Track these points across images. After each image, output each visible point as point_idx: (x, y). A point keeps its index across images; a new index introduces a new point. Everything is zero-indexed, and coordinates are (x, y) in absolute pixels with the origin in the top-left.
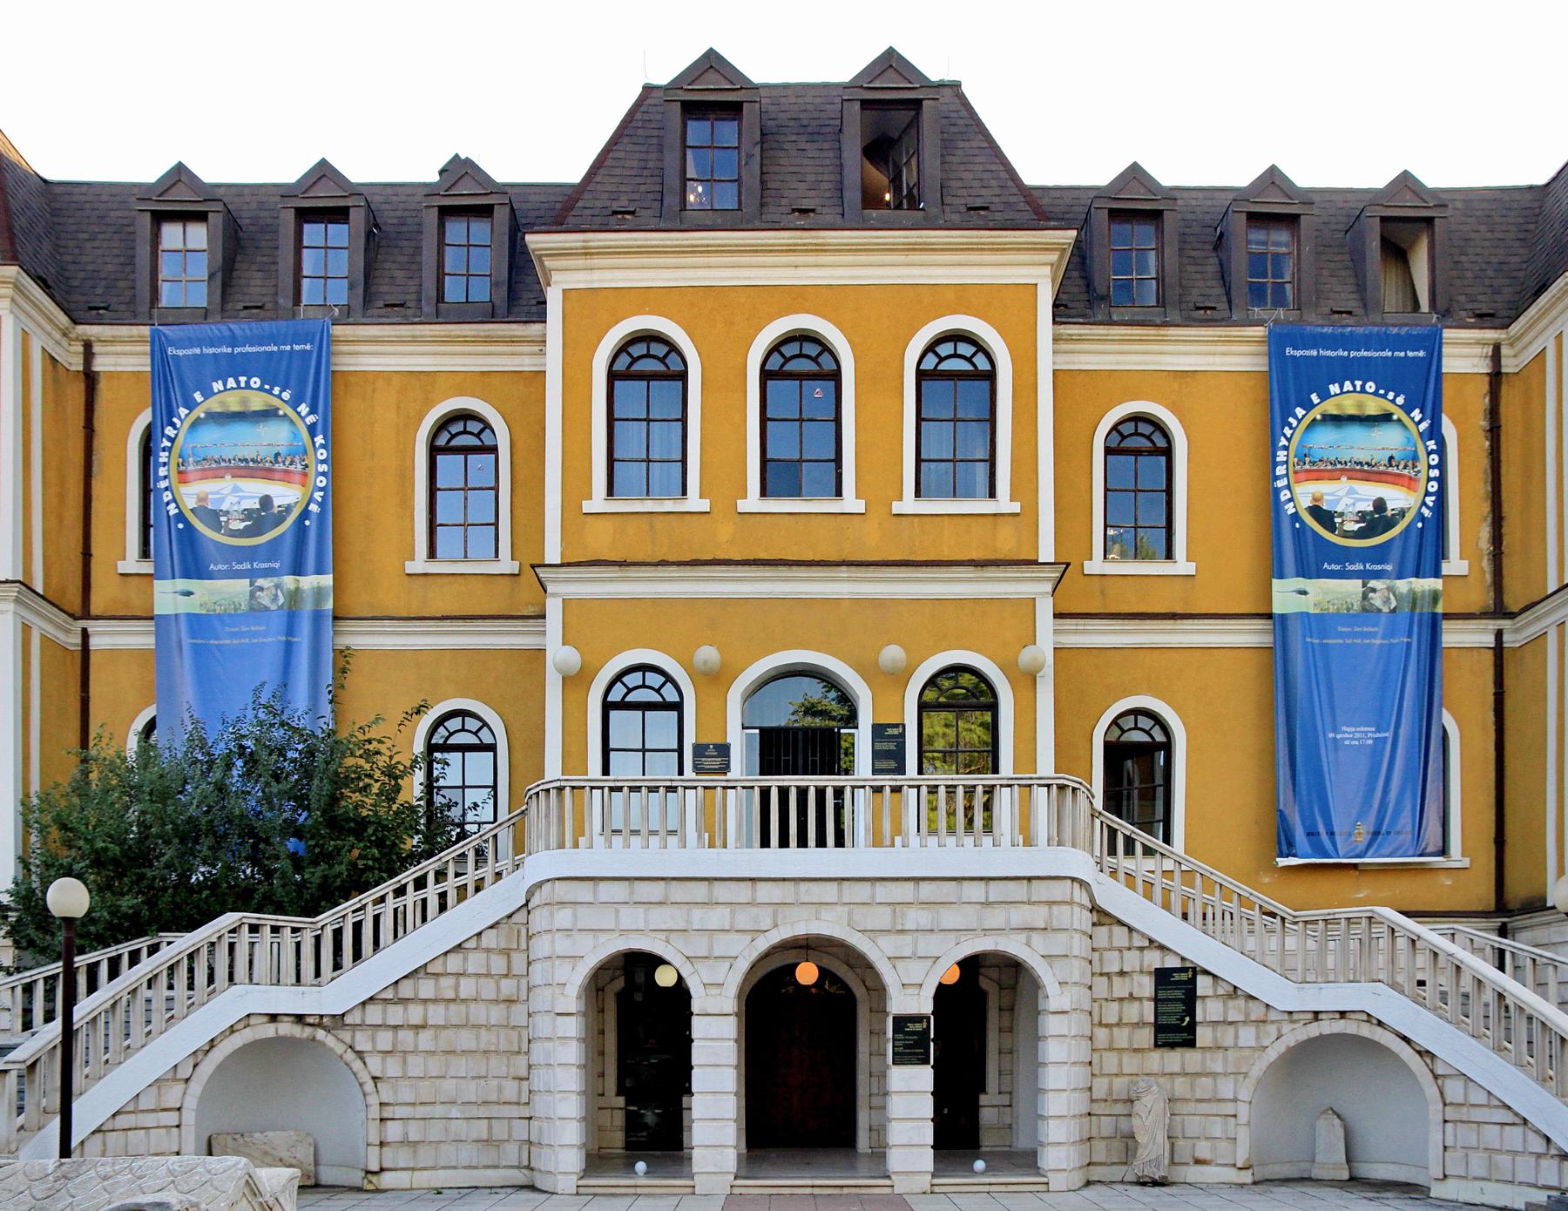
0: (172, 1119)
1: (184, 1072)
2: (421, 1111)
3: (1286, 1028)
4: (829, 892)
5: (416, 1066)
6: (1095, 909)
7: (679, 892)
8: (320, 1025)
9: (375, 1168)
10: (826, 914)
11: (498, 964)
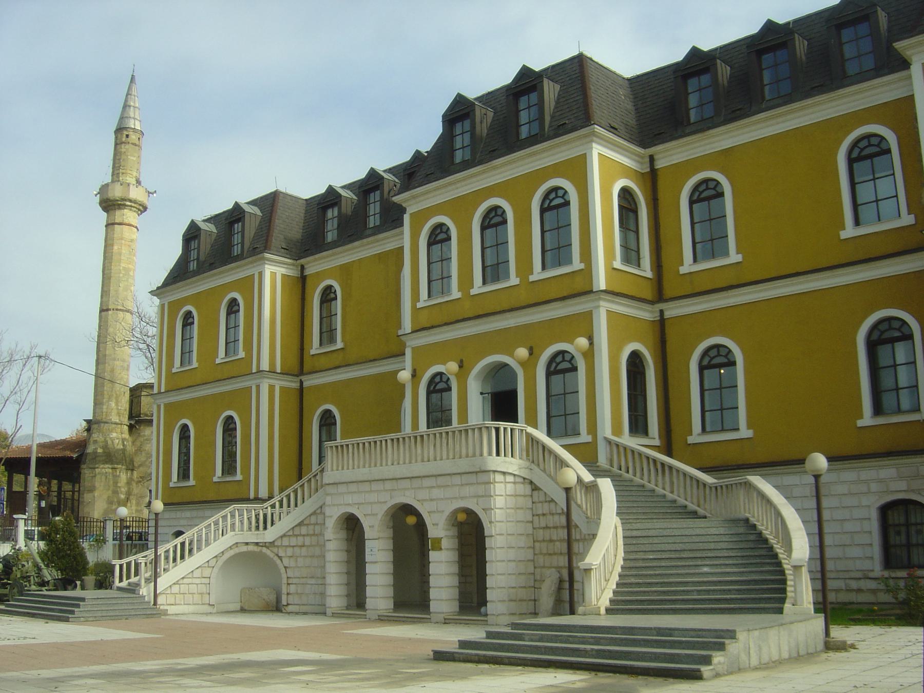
0: (207, 581)
1: (212, 563)
10: (407, 493)
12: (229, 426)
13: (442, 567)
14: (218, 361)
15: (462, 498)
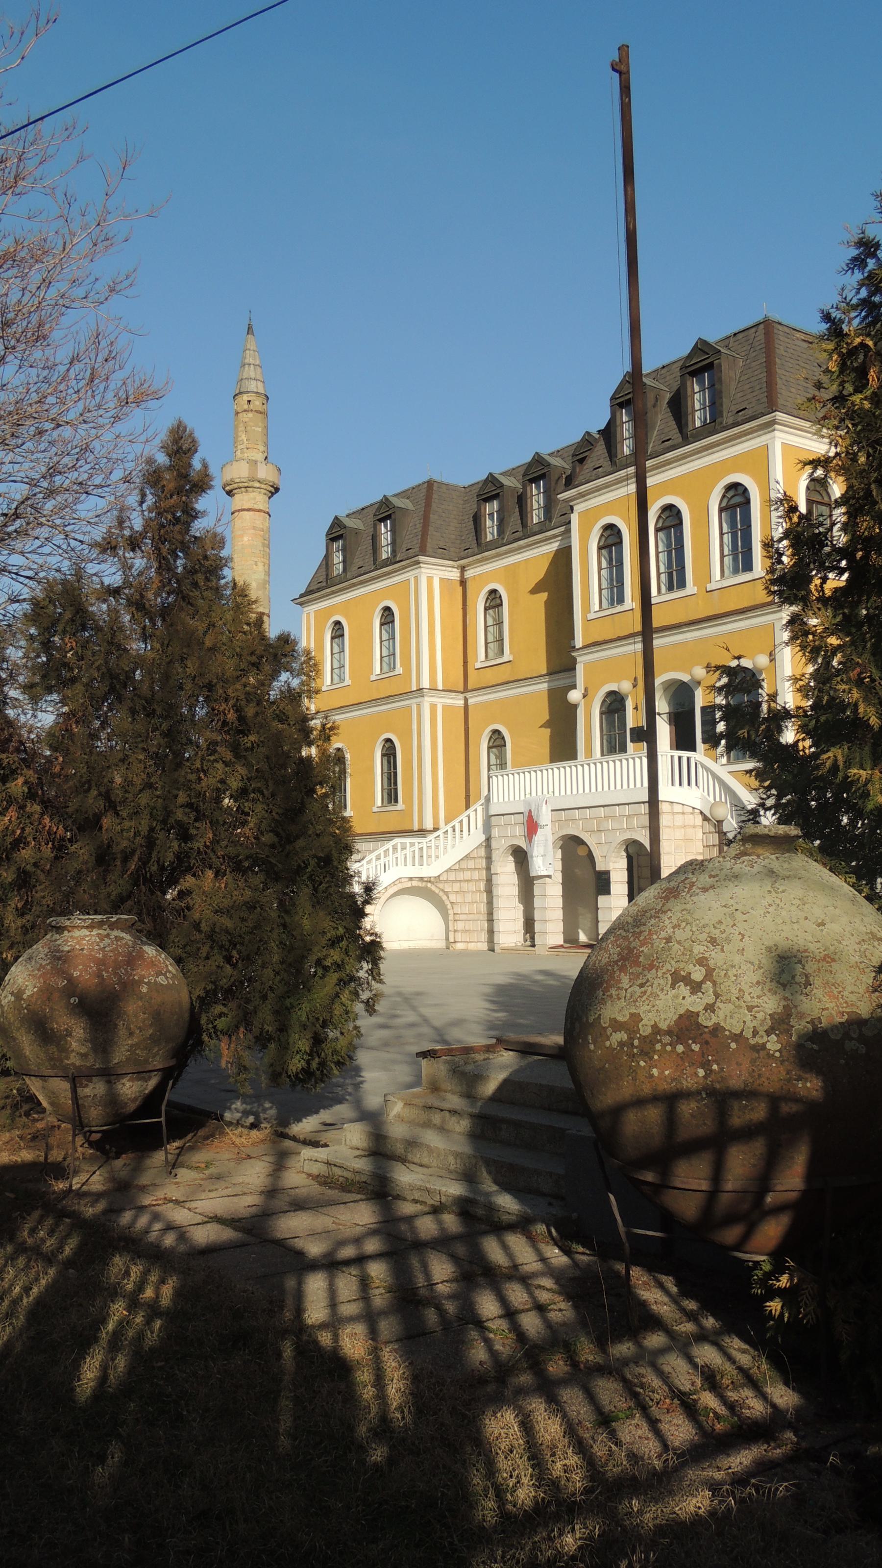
12: (389, 752)
14: (373, 678)
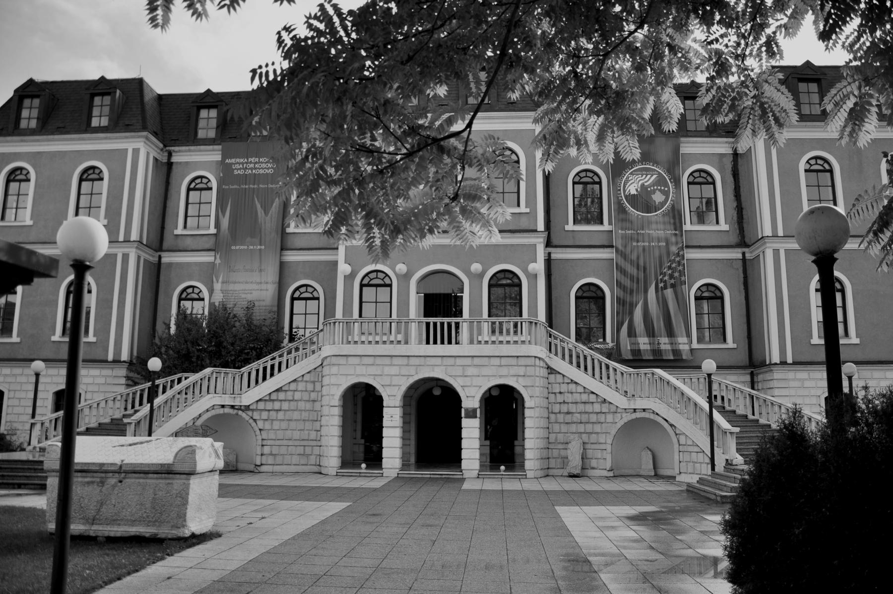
2: (278, 443)
3: (624, 415)
4: (438, 361)
5: (276, 425)
6: (549, 367)
7: (379, 361)
8: (240, 409)
9: (259, 463)
11: (310, 387)
13: (471, 432)
15: (501, 376)
